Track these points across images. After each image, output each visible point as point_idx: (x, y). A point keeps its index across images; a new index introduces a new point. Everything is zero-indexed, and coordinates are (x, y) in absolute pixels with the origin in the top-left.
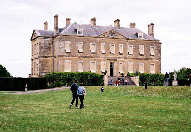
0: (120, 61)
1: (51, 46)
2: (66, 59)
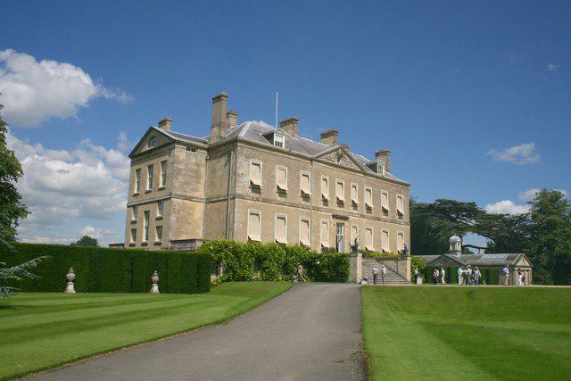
2: (252, 207)
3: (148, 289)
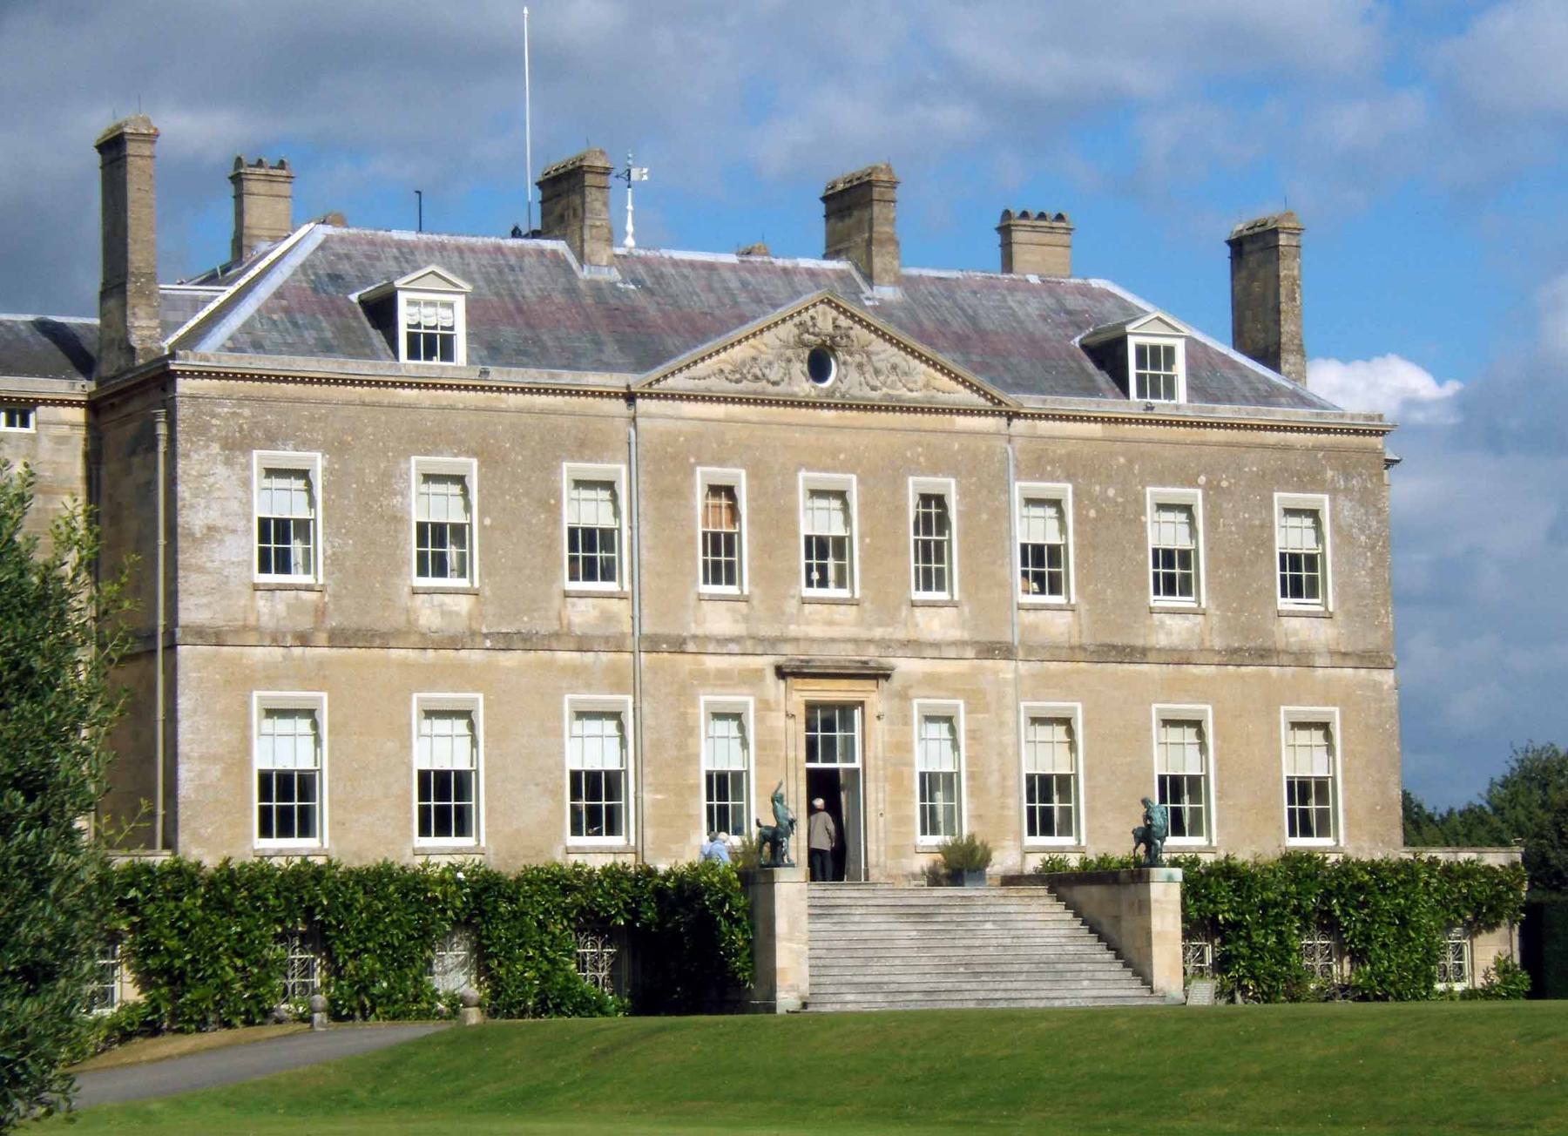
2: (272, 678)
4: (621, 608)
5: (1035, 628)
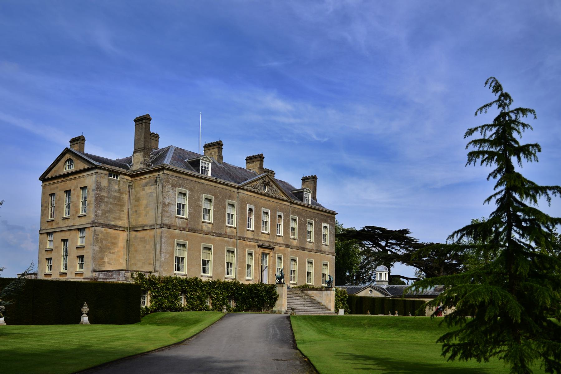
0: (279, 250)
1: (125, 197)
2: (178, 238)
3: (77, 320)
4: (234, 230)
5: (292, 243)
